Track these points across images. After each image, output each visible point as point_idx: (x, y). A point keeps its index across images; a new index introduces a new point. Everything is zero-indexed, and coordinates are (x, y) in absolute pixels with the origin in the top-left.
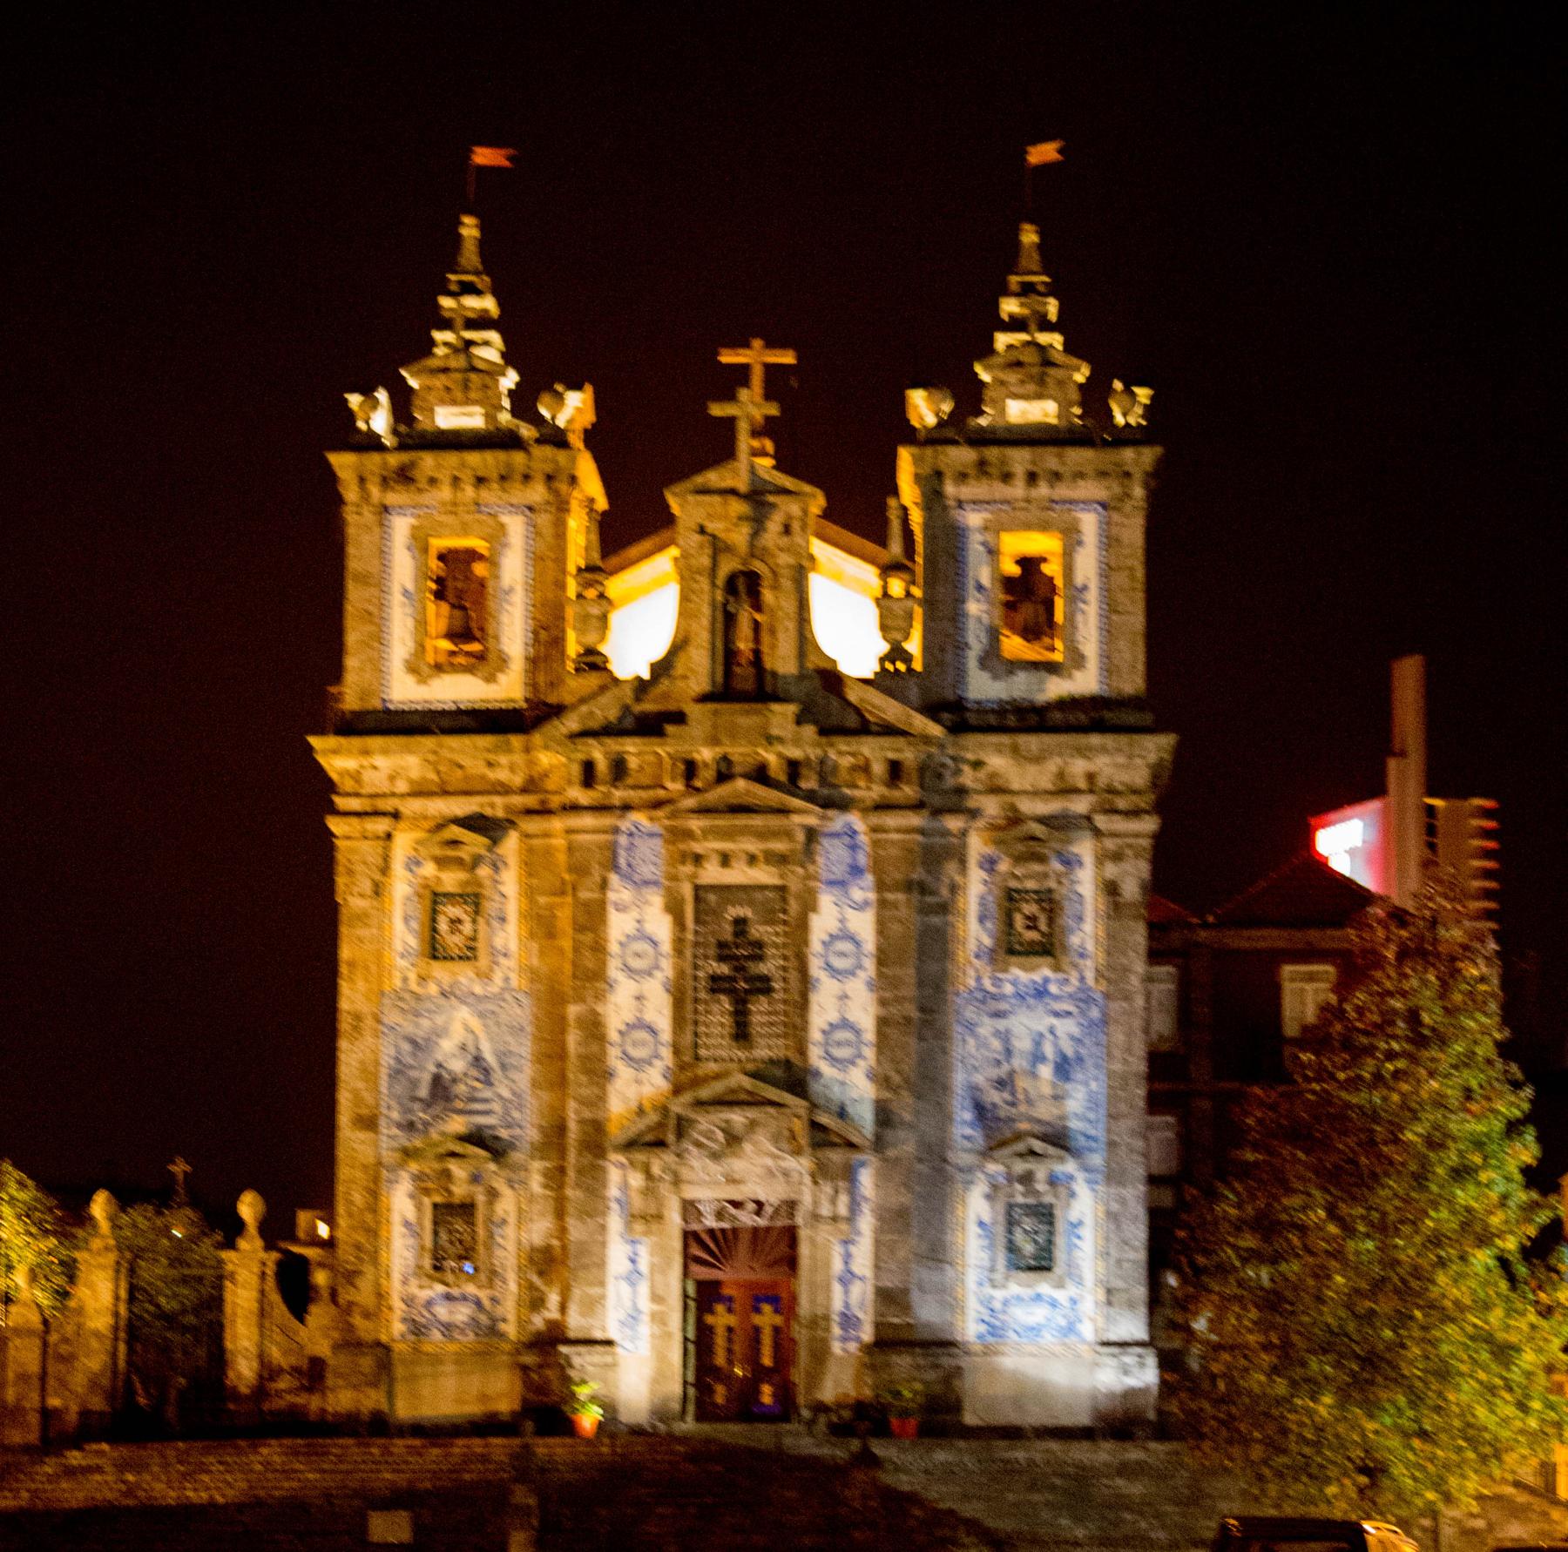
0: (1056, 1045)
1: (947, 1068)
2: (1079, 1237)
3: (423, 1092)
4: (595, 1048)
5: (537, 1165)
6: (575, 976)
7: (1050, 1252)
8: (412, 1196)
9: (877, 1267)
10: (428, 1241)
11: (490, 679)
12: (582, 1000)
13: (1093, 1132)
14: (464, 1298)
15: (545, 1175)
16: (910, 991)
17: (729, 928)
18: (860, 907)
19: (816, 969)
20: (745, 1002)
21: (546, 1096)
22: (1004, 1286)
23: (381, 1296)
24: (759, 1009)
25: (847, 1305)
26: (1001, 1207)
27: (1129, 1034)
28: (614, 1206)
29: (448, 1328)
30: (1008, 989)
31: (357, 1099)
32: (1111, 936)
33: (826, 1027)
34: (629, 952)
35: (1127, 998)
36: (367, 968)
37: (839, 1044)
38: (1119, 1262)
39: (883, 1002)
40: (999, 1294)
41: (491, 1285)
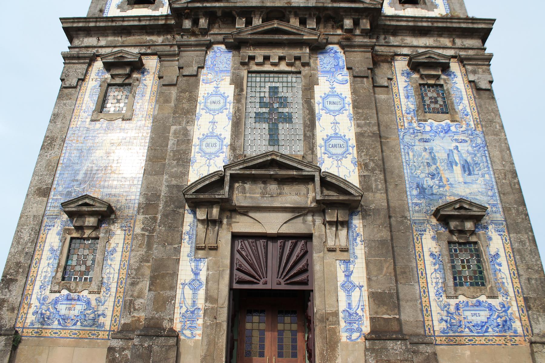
0: (461, 156)
1: (401, 167)
2: (500, 265)
3: (80, 177)
4: (183, 147)
5: (141, 217)
6: (175, 113)
7: (481, 272)
8: (58, 234)
9: (369, 279)
10: (63, 263)
11: (156, 9)
12: (180, 124)
13: (491, 202)
14: (79, 299)
15: (143, 223)
16: (374, 121)
17: (267, 90)
18: (343, 83)
19: (318, 109)
20: (276, 124)
21: (152, 178)
22: (457, 297)
23: (24, 295)
24: (283, 128)
25: (349, 304)
26: (445, 244)
27: (501, 151)
28: (187, 237)
29: (65, 319)
30: (428, 129)
31: (41, 181)
32: (479, 107)
33: (325, 137)
34: (209, 101)
35: (497, 135)
36: (65, 117)
37: (334, 146)
38: (529, 279)
39: (358, 126)
40: (453, 302)
41: (99, 293)
